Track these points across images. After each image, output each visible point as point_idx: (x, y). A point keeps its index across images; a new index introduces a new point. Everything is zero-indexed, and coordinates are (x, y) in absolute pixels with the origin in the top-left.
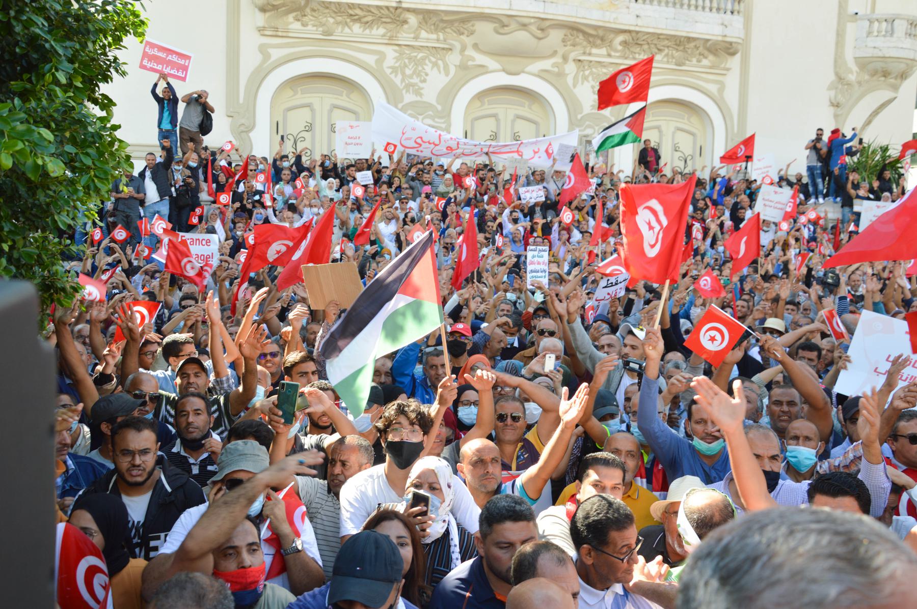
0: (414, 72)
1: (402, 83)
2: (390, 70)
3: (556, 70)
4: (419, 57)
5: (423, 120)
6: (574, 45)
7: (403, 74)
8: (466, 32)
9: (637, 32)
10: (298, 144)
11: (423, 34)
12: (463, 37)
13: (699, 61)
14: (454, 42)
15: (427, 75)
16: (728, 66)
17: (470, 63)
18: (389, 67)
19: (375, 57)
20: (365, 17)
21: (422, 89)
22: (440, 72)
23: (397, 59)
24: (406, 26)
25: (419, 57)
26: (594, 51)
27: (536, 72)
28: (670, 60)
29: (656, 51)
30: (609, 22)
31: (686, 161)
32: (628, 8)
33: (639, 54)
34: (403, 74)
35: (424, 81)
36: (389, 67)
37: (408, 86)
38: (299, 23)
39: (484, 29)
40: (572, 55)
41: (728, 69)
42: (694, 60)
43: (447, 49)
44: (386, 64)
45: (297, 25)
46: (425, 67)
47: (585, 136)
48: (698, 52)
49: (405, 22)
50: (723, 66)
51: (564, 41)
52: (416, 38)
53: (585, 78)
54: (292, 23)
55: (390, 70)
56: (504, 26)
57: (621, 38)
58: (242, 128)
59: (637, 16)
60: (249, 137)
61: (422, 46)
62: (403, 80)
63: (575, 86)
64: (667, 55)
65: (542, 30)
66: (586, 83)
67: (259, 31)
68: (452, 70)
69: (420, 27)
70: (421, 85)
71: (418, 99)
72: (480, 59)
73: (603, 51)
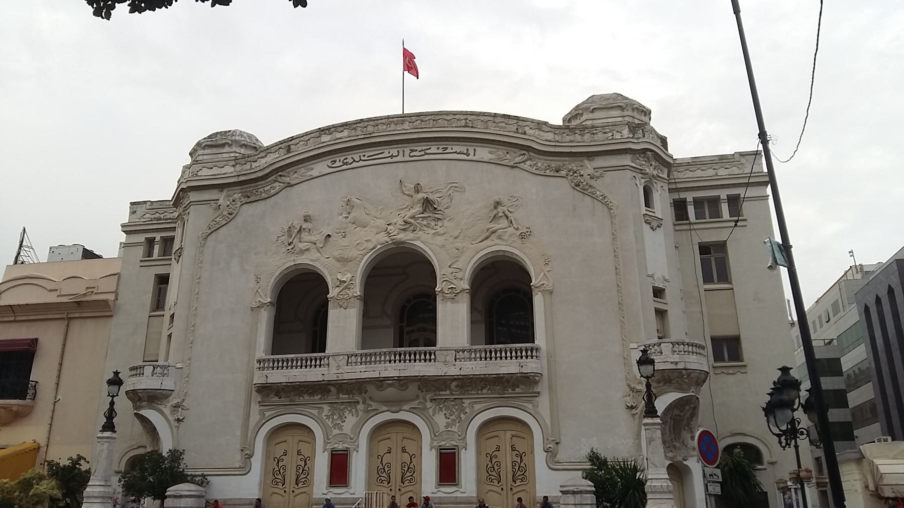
0: (338, 418)
1: (332, 424)
2: (326, 417)
3: (420, 406)
4: (341, 408)
5: (343, 444)
6: (427, 391)
7: (333, 419)
8: (363, 391)
9: (463, 379)
10: (280, 462)
11: (341, 396)
12: (363, 395)
13: (514, 390)
14: (357, 398)
15: (346, 418)
16: (534, 391)
17: (369, 409)
18: (325, 416)
19: (318, 411)
20: (308, 391)
21: (343, 426)
22: (353, 416)
23: (329, 411)
24: (331, 393)
25: (341, 408)
26: (441, 393)
27: (408, 409)
28: (493, 392)
29: (481, 388)
30: (441, 376)
31: (521, 458)
32: (454, 365)
33: (471, 391)
34: (333, 419)
35: (344, 421)
36: (325, 416)
37: (336, 426)
38: (277, 397)
39: (371, 389)
40: (428, 397)
41: (539, 393)
42: (510, 391)
43: (356, 402)
44: (323, 414)
45: (276, 399)
46: (345, 414)
47: (440, 446)
48: (510, 384)
49: (331, 391)
50: (531, 391)
51: (419, 389)
52: (338, 398)
53: (441, 409)
54: (274, 397)
55: (326, 417)
56: (381, 386)
57: (454, 383)
58: (247, 456)
59: (460, 369)
60: (250, 461)
61: (342, 402)
62: (332, 422)
63: (433, 416)
64: (489, 390)
65: (402, 386)
66: (440, 412)
67: (259, 403)
68: (360, 413)
69: (338, 392)
70: (341, 423)
71: (340, 432)
72: (374, 405)
73: (448, 392)
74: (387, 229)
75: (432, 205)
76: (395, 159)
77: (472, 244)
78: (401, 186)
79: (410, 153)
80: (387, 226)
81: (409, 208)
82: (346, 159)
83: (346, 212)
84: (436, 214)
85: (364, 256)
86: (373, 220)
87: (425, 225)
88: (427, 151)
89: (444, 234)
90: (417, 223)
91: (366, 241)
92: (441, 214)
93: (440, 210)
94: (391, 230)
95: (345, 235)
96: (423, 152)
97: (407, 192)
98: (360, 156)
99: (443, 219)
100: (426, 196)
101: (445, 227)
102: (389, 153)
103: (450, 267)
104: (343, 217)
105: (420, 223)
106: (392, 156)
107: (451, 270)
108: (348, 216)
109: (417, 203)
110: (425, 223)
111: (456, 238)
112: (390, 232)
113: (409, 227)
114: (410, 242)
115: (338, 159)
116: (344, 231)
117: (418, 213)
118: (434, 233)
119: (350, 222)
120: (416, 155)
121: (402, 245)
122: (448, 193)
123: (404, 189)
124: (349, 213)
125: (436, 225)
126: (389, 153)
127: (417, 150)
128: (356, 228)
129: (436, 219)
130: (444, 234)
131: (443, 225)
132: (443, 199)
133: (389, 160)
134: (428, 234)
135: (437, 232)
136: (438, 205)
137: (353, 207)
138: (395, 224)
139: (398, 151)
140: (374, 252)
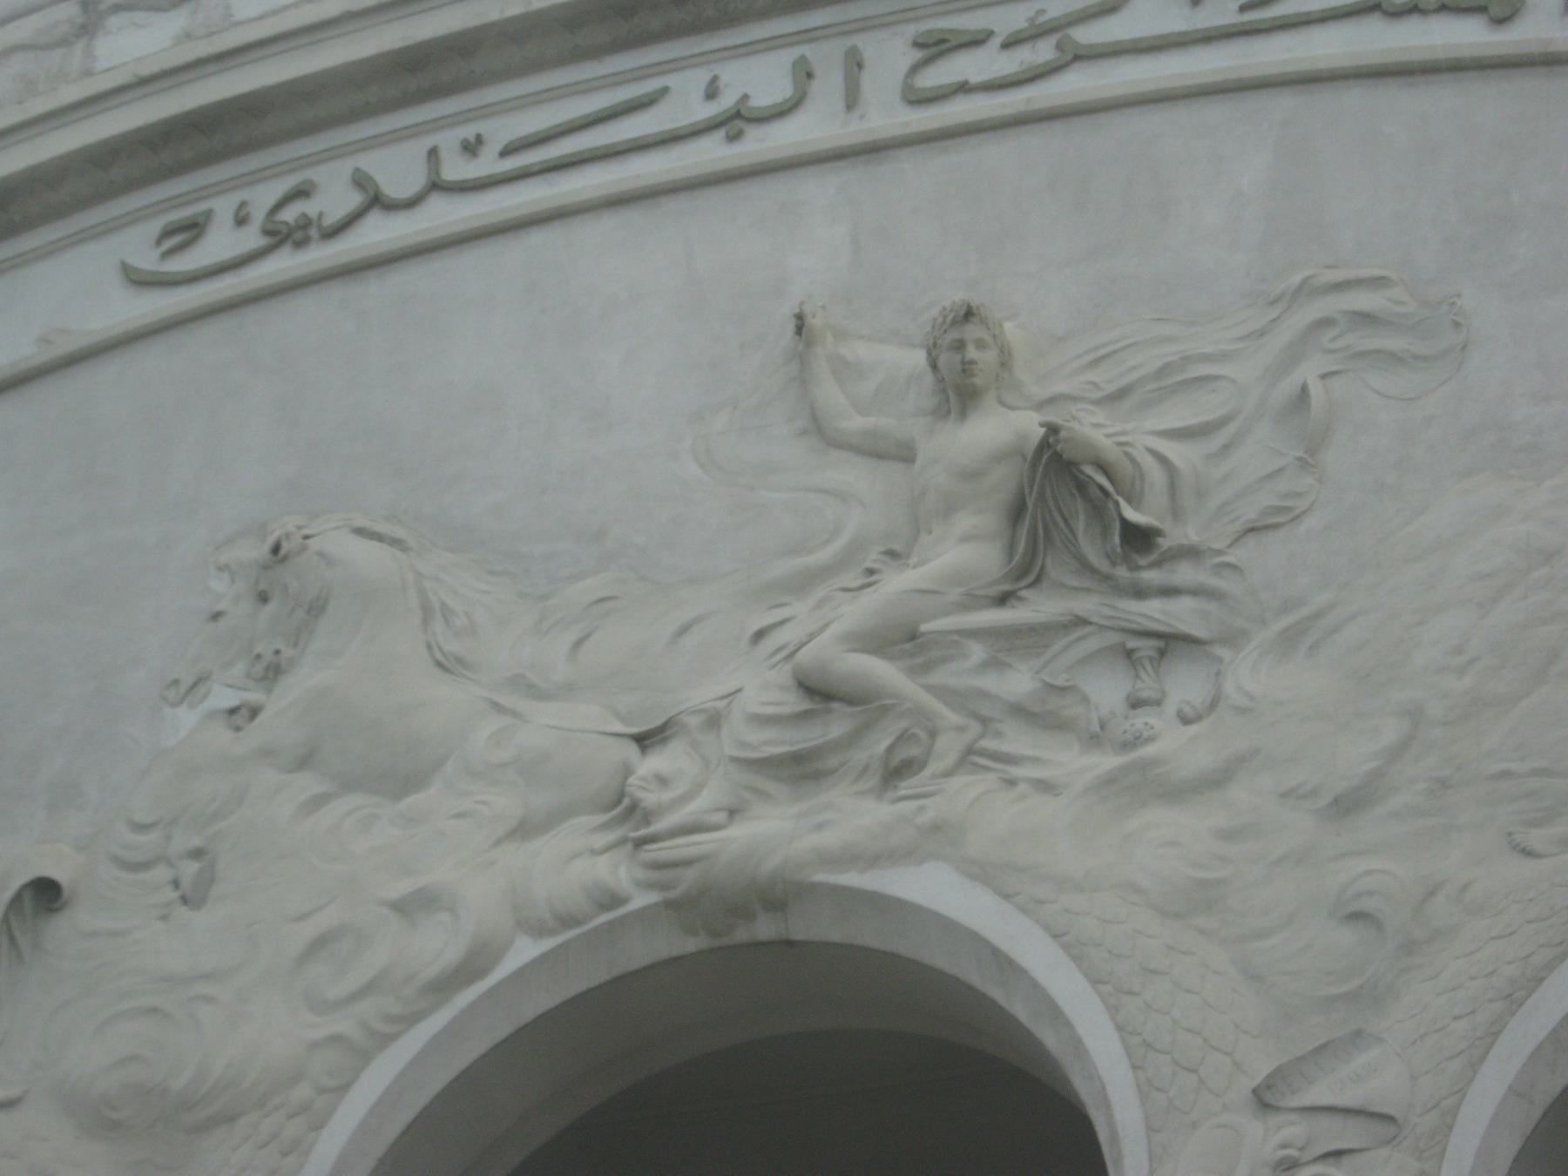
74: (628, 771)
75: (1099, 506)
76: (761, 143)
77: (1527, 853)
78: (803, 379)
79: (915, 69)
80: (632, 749)
81: (872, 558)
82: (301, 193)
83: (239, 669)
84: (1140, 593)
85: (362, 1055)
86: (498, 708)
87: (1020, 711)
88: (1086, 35)
89: (1216, 780)
90: (941, 692)
91: (402, 907)
92: (1197, 592)
93: (1191, 553)
94: (662, 781)
95: (207, 879)
96: (1052, 40)
97: (855, 423)
98: (433, 153)
99: (1233, 639)
100: (1030, 425)
101: (1241, 711)
102: (711, 93)
103: (1264, 1100)
104: (212, 715)
105: (985, 695)
106: (736, 121)
107: (1293, 1130)
108: (254, 697)
109: (949, 508)
110: (1019, 682)
111: (1347, 805)
112: (650, 798)
113: (853, 739)
114: (851, 879)
115: (224, 207)
116: (196, 842)
117: (955, 594)
118: (1110, 781)
119: (266, 753)
120: (975, 78)
121: (765, 928)
122: (1287, 387)
123: (830, 393)
124: (273, 672)
125: (1136, 704)
126: (711, 93)
127: (976, 41)
128: (317, 802)
129: (1146, 647)
130: (1216, 780)
131: (1213, 704)
132: (1227, 448)
133: (711, 153)
134: (1046, 787)
135: (1145, 765)
136: (1176, 512)
137: (317, 609)
138: (714, 721)
139: (804, 74)
140: (473, 1006)
